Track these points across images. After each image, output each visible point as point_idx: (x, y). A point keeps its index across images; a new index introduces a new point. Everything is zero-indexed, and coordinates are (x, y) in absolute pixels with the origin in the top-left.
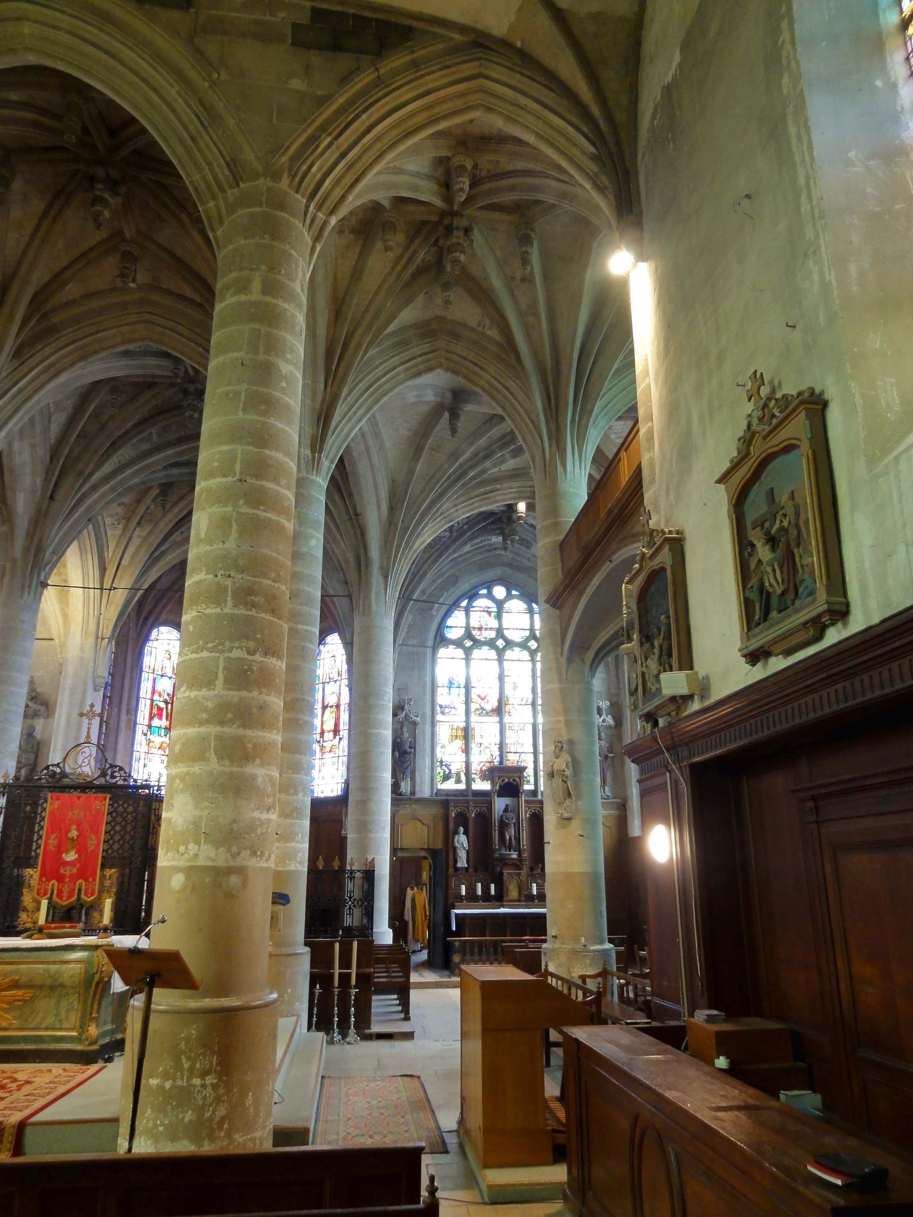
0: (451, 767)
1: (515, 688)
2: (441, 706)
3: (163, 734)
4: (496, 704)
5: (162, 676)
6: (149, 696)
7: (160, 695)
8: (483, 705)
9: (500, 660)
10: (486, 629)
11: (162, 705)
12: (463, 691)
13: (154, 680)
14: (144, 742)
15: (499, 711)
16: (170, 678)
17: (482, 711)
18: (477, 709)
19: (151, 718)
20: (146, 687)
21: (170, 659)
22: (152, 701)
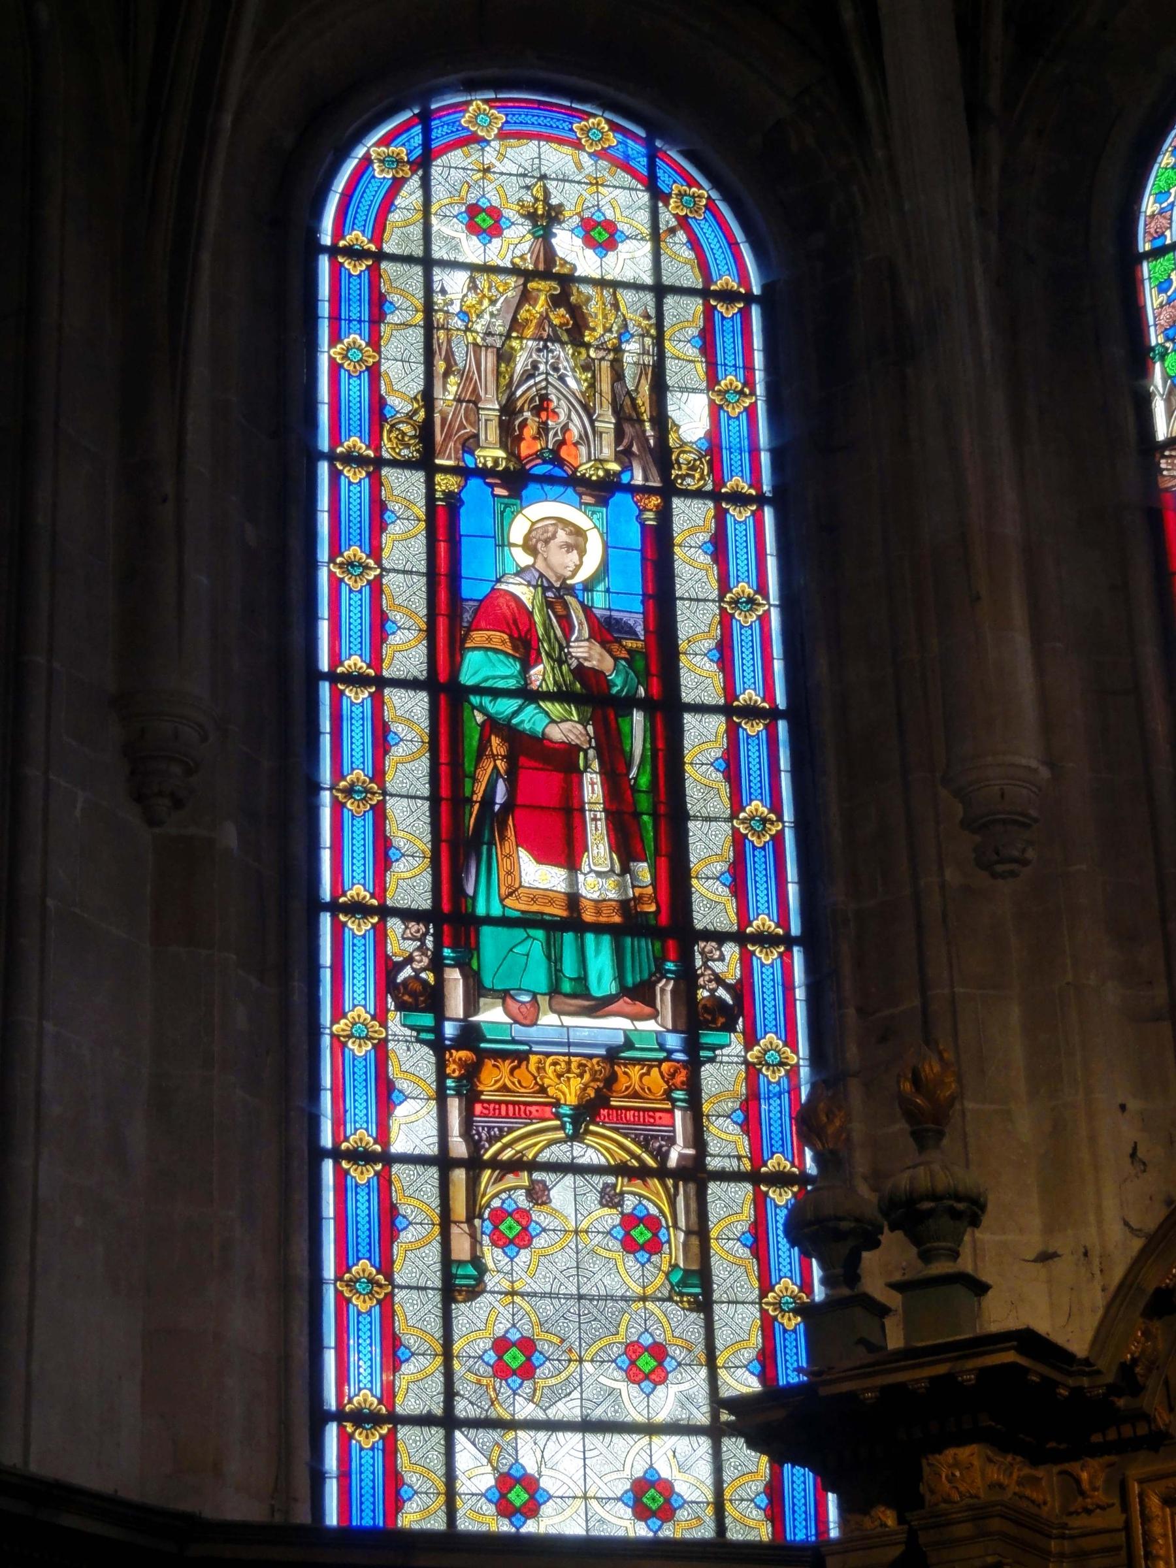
3: (602, 980)
5: (516, 481)
6: (407, 653)
7: (525, 648)
11: (564, 726)
13: (442, 522)
14: (413, 1064)
16: (602, 490)
19: (460, 842)
20: (371, 589)
21: (576, 332)
22: (445, 690)
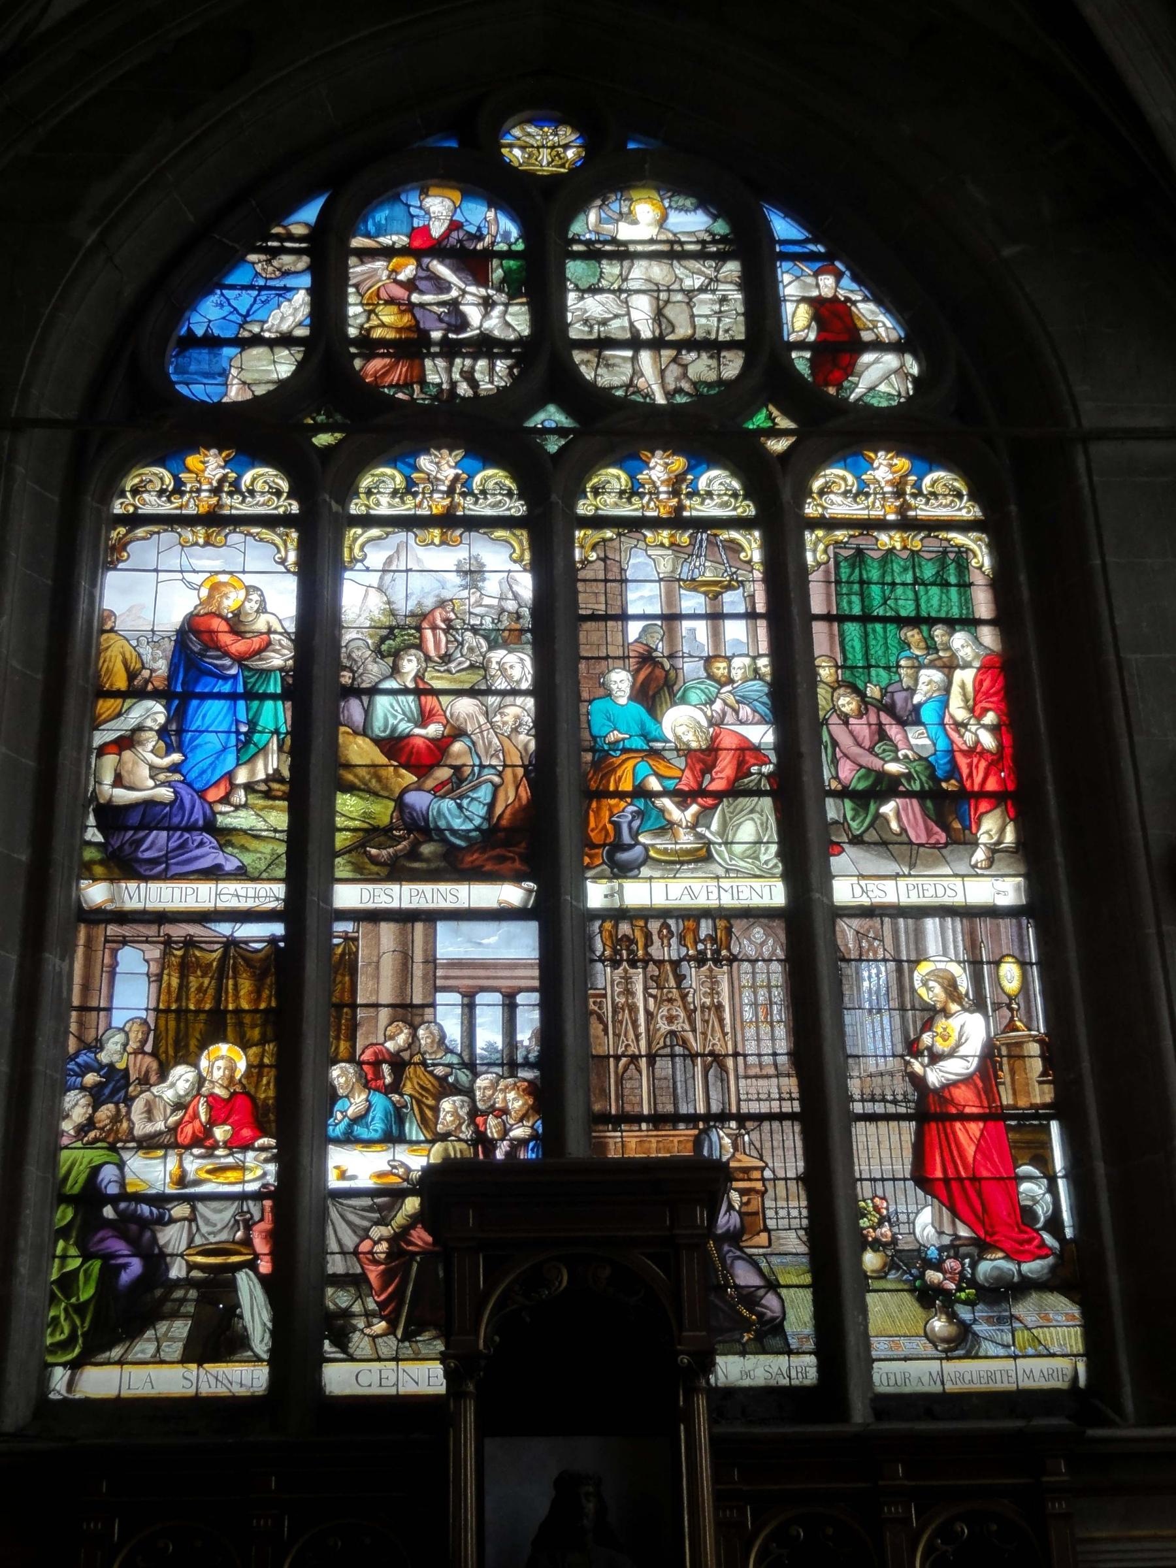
0: (172, 1237)
1: (657, 686)
2: (112, 817)
4: (515, 794)
8: (418, 800)
9: (546, 528)
10: (450, 350)
12: (275, 715)
15: (547, 830)
17: (410, 848)
18: (371, 834)
